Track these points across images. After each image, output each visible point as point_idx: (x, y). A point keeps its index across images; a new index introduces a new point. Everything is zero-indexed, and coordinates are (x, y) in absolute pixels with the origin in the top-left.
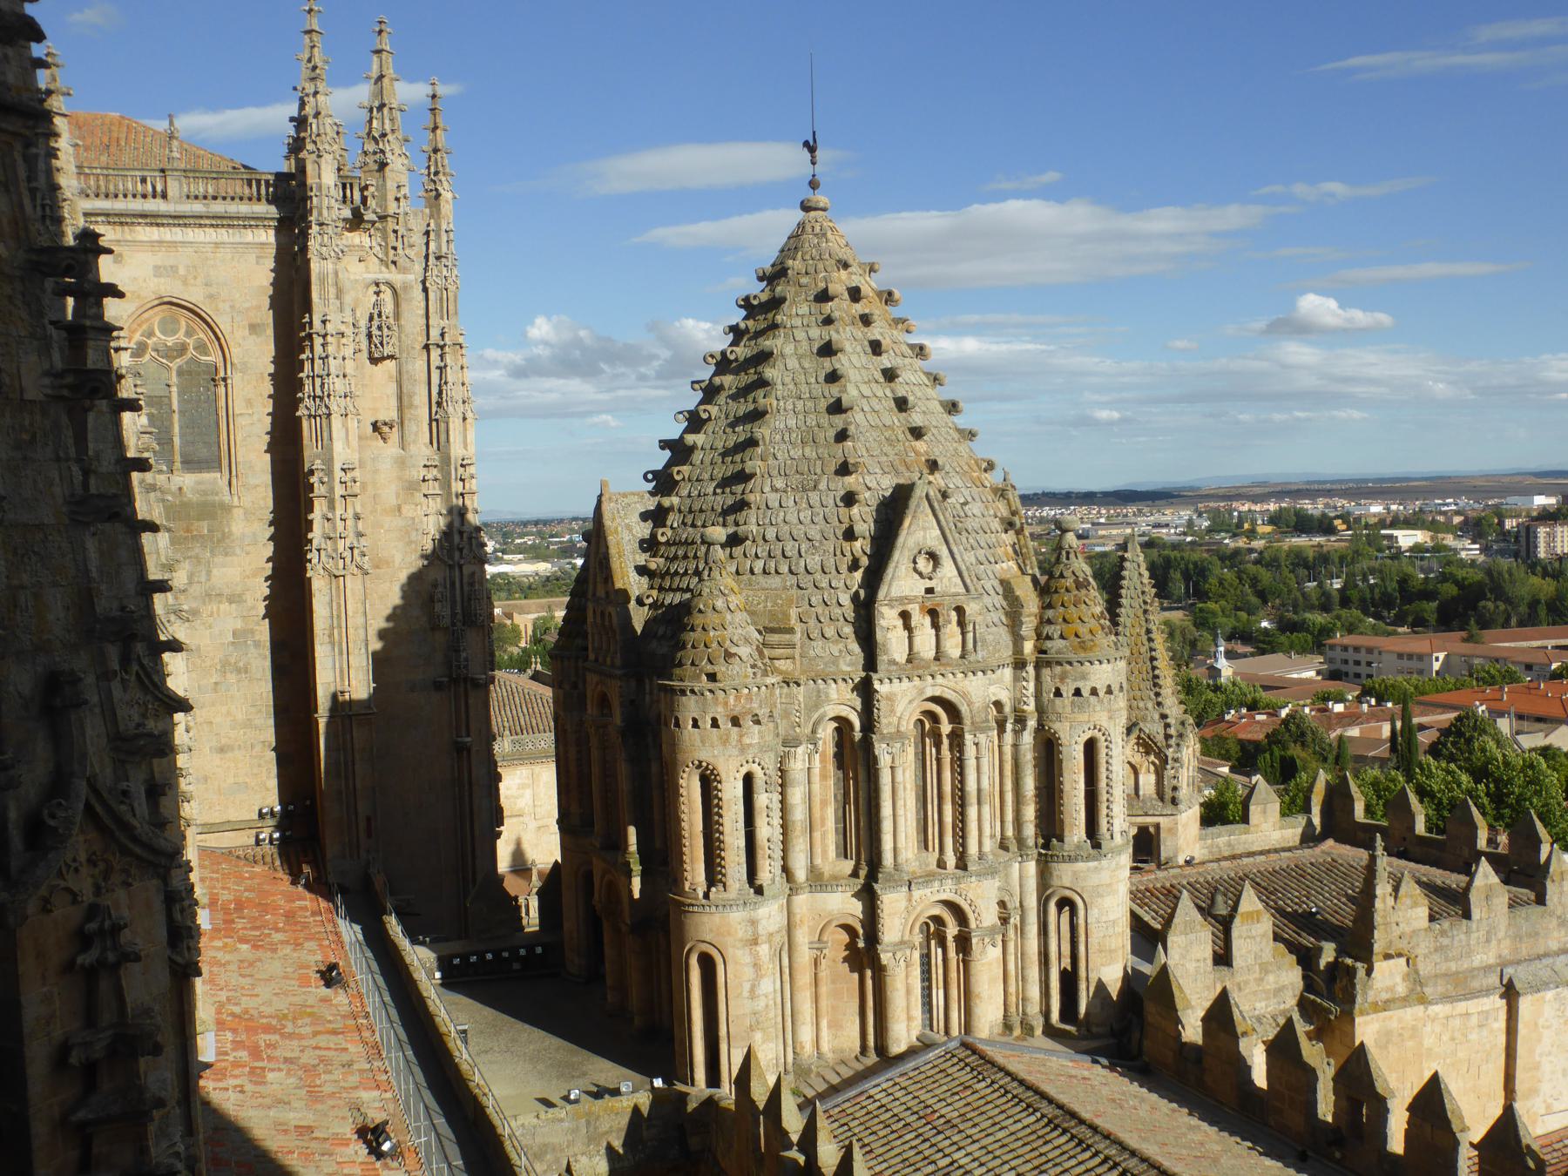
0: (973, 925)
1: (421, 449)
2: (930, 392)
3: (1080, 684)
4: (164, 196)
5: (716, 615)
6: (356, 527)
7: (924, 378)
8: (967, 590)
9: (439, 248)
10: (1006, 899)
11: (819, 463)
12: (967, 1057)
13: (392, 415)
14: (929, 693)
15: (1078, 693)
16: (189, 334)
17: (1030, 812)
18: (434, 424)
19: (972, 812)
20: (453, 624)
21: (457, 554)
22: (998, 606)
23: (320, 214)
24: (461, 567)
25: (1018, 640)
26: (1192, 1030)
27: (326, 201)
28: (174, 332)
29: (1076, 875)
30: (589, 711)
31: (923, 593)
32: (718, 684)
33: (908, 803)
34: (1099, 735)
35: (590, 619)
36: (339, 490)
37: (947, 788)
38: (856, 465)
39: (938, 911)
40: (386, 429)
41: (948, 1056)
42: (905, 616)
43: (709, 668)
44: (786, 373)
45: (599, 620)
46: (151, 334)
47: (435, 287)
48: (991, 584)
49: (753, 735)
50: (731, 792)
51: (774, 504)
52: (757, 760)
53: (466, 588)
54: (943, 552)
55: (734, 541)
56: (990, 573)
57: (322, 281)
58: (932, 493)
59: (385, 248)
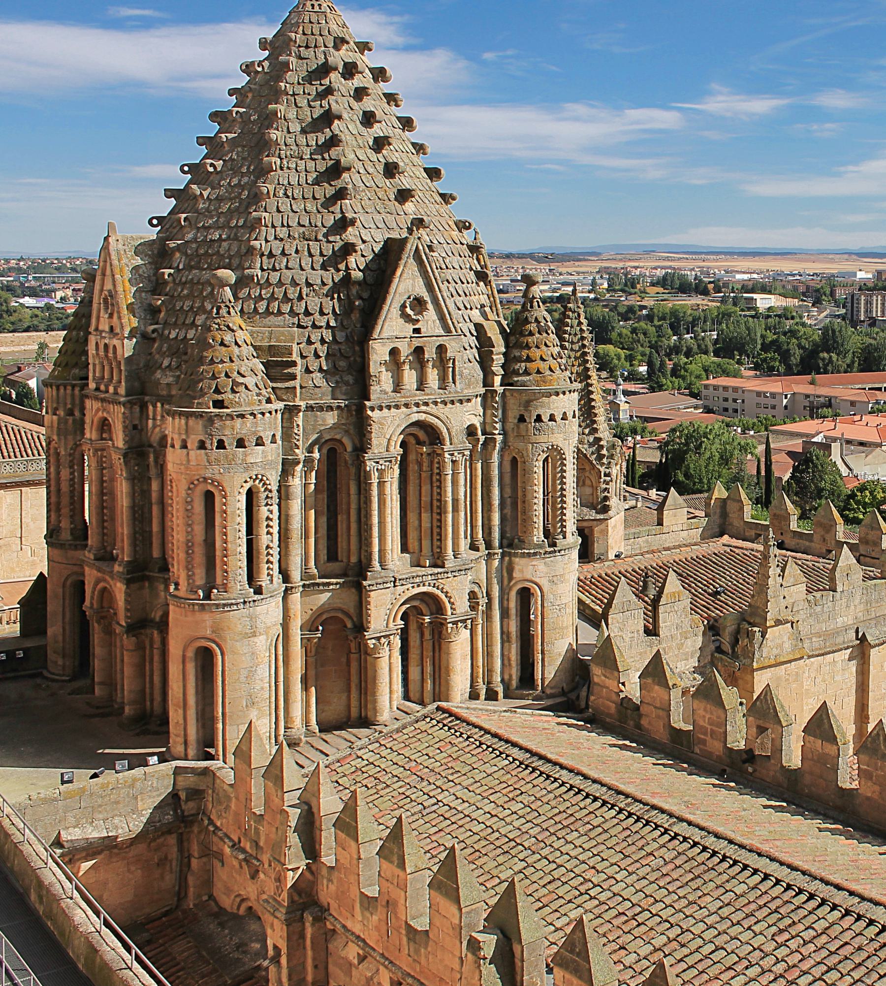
2: (415, 158)
3: (540, 411)
5: (224, 349)
7: (411, 147)
10: (476, 589)
11: (319, 216)
12: (443, 719)
15: (539, 419)
22: (473, 345)
30: (88, 435)
33: (394, 512)
35: (92, 349)
37: (425, 499)
38: (353, 222)
39: (416, 603)
41: (428, 720)
44: (289, 135)
45: (102, 353)
49: (256, 454)
51: (277, 252)
52: (260, 477)
55: (243, 282)
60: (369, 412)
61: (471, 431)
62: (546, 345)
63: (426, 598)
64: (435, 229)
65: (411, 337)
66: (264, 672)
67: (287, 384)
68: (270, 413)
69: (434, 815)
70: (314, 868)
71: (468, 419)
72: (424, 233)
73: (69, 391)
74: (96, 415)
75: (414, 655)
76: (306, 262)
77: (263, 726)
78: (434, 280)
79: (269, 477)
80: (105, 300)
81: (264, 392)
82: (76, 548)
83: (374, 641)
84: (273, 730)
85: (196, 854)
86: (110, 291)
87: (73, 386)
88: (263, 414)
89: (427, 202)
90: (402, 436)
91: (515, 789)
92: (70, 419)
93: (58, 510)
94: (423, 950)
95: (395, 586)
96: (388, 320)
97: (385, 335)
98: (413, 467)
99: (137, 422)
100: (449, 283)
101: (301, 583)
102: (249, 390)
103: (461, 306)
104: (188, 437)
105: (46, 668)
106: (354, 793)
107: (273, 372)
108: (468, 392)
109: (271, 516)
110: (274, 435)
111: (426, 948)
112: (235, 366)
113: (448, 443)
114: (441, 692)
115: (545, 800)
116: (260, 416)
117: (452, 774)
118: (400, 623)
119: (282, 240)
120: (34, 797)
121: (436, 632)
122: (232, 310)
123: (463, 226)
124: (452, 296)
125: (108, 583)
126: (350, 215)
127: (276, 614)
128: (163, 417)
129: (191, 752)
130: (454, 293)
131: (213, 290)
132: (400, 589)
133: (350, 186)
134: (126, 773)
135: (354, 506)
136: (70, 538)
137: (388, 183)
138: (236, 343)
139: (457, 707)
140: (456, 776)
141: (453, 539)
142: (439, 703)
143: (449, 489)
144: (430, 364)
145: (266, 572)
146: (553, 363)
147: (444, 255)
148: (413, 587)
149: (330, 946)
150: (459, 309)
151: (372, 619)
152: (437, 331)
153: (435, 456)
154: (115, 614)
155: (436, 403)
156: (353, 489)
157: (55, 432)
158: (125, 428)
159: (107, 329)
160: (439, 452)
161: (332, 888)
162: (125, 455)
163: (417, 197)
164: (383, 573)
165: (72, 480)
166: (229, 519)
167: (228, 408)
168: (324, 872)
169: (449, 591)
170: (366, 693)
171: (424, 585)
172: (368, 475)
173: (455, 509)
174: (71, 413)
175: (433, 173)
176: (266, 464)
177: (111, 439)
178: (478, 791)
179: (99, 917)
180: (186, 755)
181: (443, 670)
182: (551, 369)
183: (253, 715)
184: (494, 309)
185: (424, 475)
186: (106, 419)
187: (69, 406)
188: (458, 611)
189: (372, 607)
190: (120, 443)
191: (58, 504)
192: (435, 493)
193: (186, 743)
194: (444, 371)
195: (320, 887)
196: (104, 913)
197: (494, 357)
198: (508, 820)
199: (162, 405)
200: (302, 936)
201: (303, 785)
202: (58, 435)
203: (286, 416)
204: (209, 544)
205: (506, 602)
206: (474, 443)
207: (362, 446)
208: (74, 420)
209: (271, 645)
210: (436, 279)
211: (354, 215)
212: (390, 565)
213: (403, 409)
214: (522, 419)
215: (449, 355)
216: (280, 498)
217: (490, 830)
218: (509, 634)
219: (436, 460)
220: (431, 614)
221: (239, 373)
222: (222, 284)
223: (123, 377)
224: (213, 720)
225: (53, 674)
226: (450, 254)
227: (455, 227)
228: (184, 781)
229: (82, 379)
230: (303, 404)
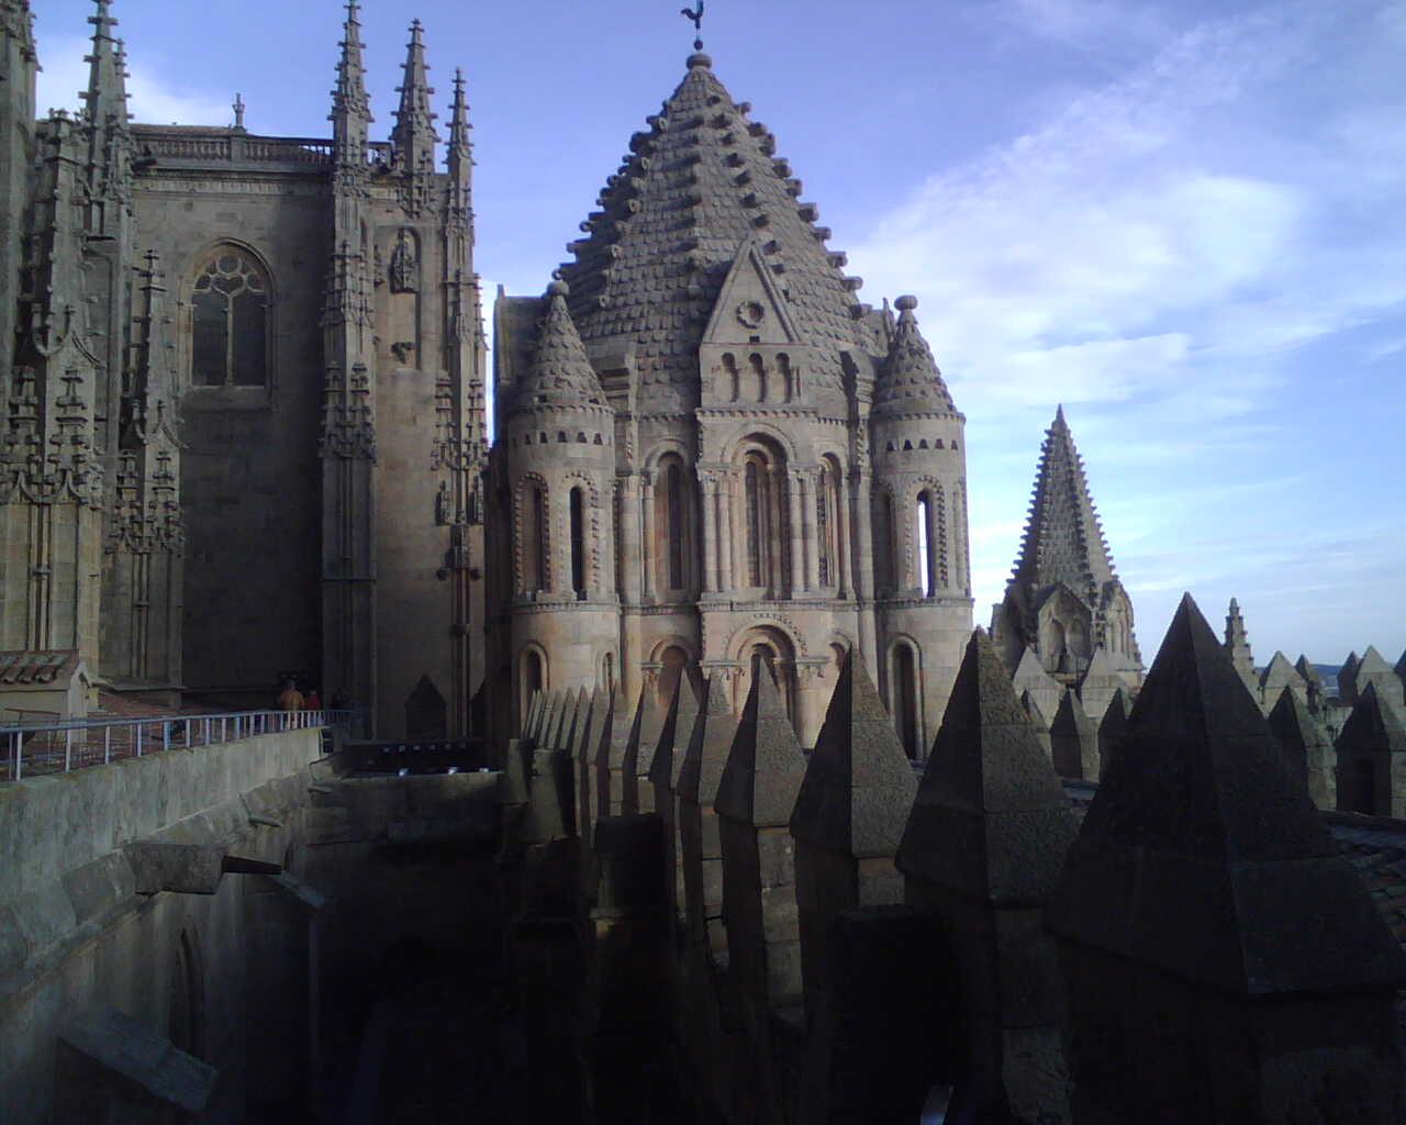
0: (799, 652)
1: (433, 367)
4: (229, 157)
6: (364, 418)
8: (791, 339)
9: (457, 203)
13: (412, 339)
14: (753, 429)
15: (908, 446)
16: (244, 272)
17: (867, 563)
18: (448, 351)
19: (797, 544)
20: (457, 521)
21: (464, 460)
23: (345, 159)
24: (467, 471)
25: (852, 402)
27: (349, 151)
28: (232, 269)
29: (910, 622)
31: (748, 340)
32: (546, 404)
34: (930, 486)
36: (350, 386)
37: (776, 525)
39: (764, 640)
40: (404, 350)
42: (729, 359)
43: (543, 392)
46: (213, 271)
50: (560, 501)
52: (582, 474)
53: (471, 490)
54: (765, 303)
57: (345, 213)
58: (755, 252)
59: (410, 202)
62: (918, 368)
76: (651, 283)
110: (598, 436)
116: (581, 410)
132: (738, 615)
137: (745, 214)
164: (719, 596)
173: (805, 537)
176: (588, 461)
221: (563, 370)
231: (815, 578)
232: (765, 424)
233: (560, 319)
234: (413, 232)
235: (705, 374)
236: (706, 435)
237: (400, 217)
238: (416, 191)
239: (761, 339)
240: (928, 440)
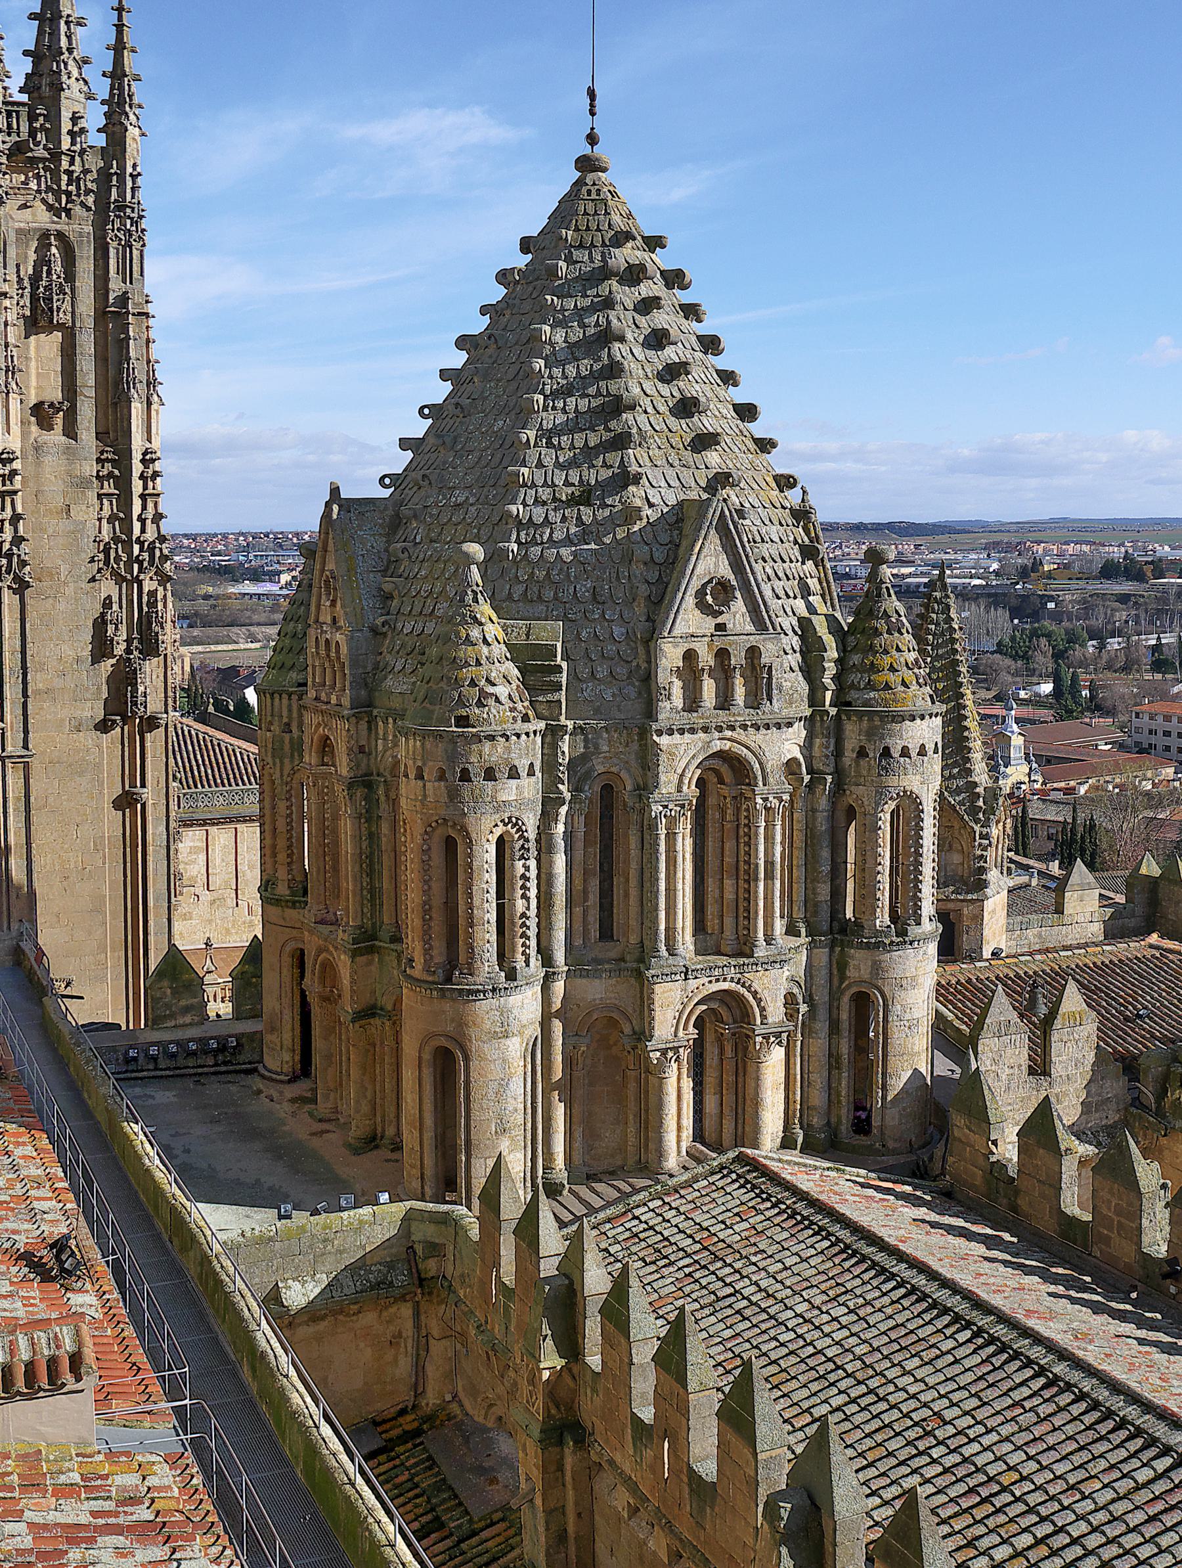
3: (889, 742)
10: (796, 990)
26: (1008, 1149)
31: (713, 630)
39: (714, 1005)
47: (115, 244)
48: (788, 622)
49: (509, 791)
52: (514, 820)
56: (788, 610)
59: (57, 194)
60: (655, 737)
61: (791, 766)
63: (728, 999)
64: (746, 487)
65: (712, 635)
66: (517, 1088)
67: (549, 697)
68: (527, 734)
69: (729, 1311)
70: (575, 1370)
71: (789, 751)
72: (731, 492)
73: (285, 701)
74: (316, 731)
75: (710, 1079)
77: (517, 1164)
78: (744, 558)
79: (526, 820)
80: (327, 582)
81: (519, 706)
82: (294, 905)
83: (658, 1054)
84: (528, 1169)
85: (435, 1332)
86: (332, 571)
87: (290, 695)
88: (518, 736)
89: (736, 450)
90: (699, 771)
91: (838, 1284)
92: (287, 736)
93: (274, 855)
94: (708, 1510)
95: (686, 979)
96: (681, 611)
97: (676, 632)
98: (713, 815)
99: (363, 743)
100: (765, 561)
101: (566, 968)
102: (500, 703)
103: (782, 594)
104: (424, 764)
105: (261, 1061)
106: (626, 1267)
107: (531, 680)
108: (789, 712)
109: (527, 874)
111: (712, 1508)
112: (483, 671)
113: (761, 783)
114: (747, 1132)
115: (878, 1304)
116: (514, 738)
117: (755, 1254)
118: (693, 1032)
119: (544, 503)
120: (248, 1234)
121: (740, 1046)
122: (479, 595)
123: (785, 482)
124: (769, 580)
125: (331, 954)
126: (634, 468)
127: (532, 1009)
128: (395, 736)
129: (429, 1192)
130: (772, 575)
131: (457, 570)
132: (693, 984)
133: (634, 431)
134: (352, 1213)
135: (634, 866)
136: (288, 892)
137: (684, 426)
138: (485, 641)
139: (766, 1157)
140: (760, 1256)
141: (765, 917)
142: (742, 1149)
143: (761, 848)
144: (738, 672)
145: (521, 950)
146: (909, 676)
147: (758, 522)
148: (710, 982)
149: (596, 1488)
150: (779, 598)
151: (657, 1024)
152: (748, 627)
153: (742, 800)
154: (340, 996)
155: (744, 727)
156: (634, 842)
157: (269, 754)
158: (350, 749)
159: (329, 620)
160: (749, 795)
161: (598, 1400)
162: (350, 786)
163: (723, 444)
165: (290, 815)
166: (475, 875)
167: (474, 727)
168: (589, 1378)
169: (759, 990)
170: (647, 1128)
171: (725, 980)
172: (653, 826)
173: (769, 876)
174: (287, 728)
175: (747, 412)
176: (521, 803)
177: (334, 766)
178: (788, 1283)
179: (317, 1406)
180: (423, 1194)
181: (748, 1102)
182: (904, 684)
183: (504, 1145)
184: (828, 597)
185: (728, 826)
186: (328, 738)
187: (285, 720)
188: (770, 1020)
189: (657, 1006)
190: (344, 771)
191: (274, 846)
192: (742, 853)
193: (422, 1178)
194: (756, 683)
195: (582, 1398)
196: (322, 1402)
197: (826, 665)
198: (827, 1329)
199: (395, 720)
200: (560, 1468)
201: (562, 1250)
202: (273, 757)
203: (548, 739)
204: (450, 908)
205: (835, 1011)
206: (796, 784)
207: (646, 786)
208: (291, 739)
209: (526, 1050)
210: (747, 556)
211: (639, 470)
212: (681, 950)
213: (701, 735)
214: (862, 753)
215: (763, 661)
216: (539, 851)
217: (801, 1343)
218: (838, 1058)
219: (744, 806)
220: (735, 1022)
221: (488, 680)
222: (468, 559)
223: (347, 683)
224: (454, 1147)
225: (269, 1071)
226: (767, 522)
227: (774, 485)
228: (423, 1232)
229: (300, 685)
230: (570, 724)
231: (779, 926)
232: (729, 740)
233: (476, 601)
234: (60, 236)
235: (663, 677)
236: (663, 758)
237: (40, 217)
238: (65, 178)
239: (730, 626)
240: (910, 746)
